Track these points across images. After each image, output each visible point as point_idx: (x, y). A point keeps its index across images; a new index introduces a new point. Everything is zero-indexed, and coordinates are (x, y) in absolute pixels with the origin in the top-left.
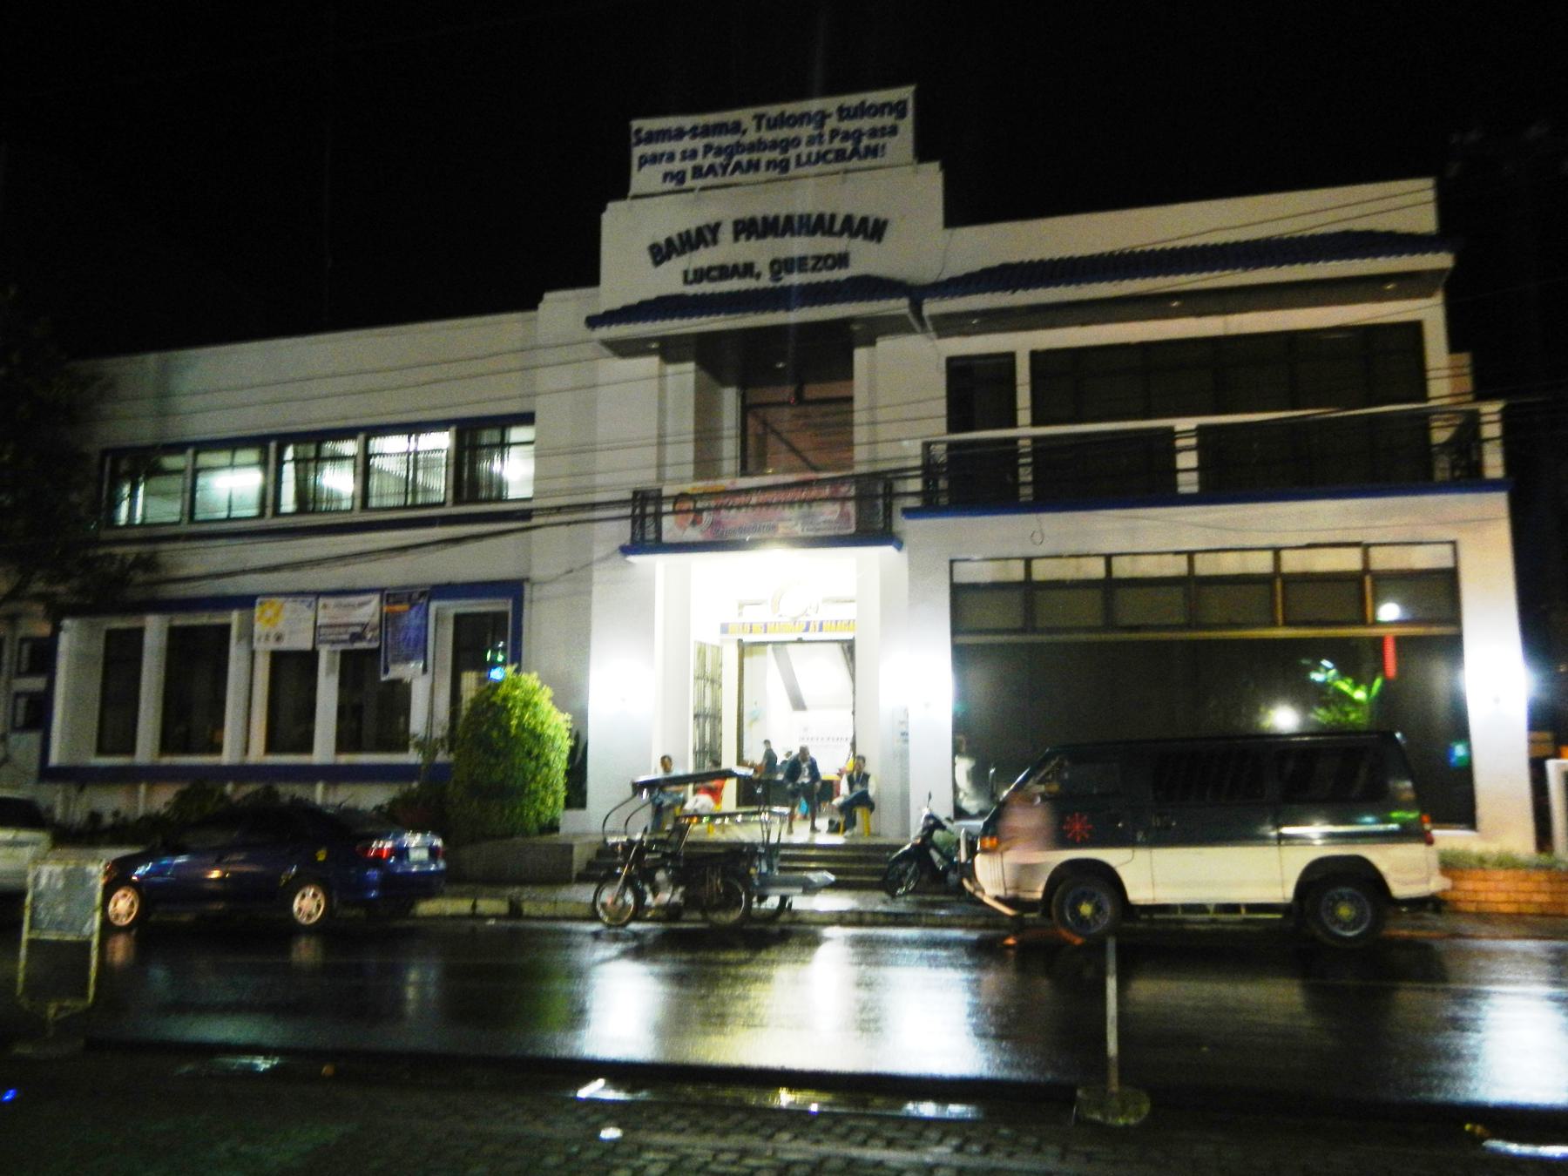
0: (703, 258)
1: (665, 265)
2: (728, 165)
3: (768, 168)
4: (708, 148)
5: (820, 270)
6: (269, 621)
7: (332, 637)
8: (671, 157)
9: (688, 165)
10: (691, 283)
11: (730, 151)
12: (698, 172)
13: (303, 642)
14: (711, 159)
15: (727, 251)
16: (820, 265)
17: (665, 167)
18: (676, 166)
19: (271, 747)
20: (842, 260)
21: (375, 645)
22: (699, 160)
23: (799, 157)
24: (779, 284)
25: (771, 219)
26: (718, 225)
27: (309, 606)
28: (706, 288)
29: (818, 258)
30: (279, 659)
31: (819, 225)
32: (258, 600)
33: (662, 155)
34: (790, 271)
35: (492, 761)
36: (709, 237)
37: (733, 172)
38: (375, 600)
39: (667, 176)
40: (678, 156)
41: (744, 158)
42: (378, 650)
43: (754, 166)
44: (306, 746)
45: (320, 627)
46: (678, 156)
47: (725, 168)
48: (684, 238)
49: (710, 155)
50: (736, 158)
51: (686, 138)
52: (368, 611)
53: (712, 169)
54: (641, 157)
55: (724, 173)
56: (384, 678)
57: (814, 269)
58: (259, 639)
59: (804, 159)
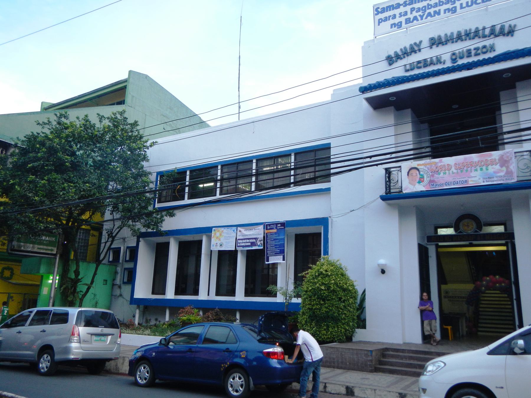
0: (414, 58)
1: (395, 65)
2: (424, 15)
3: (445, 13)
4: (412, 10)
5: (479, 54)
6: (217, 238)
8: (394, 17)
9: (403, 19)
10: (407, 71)
11: (424, 9)
12: (408, 21)
13: (230, 246)
14: (415, 14)
15: (426, 54)
16: (479, 52)
17: (392, 21)
18: (397, 21)
20: (492, 48)
21: (262, 248)
22: (409, 16)
23: (461, 4)
24: (455, 65)
25: (449, 34)
26: (421, 42)
27: (234, 231)
28: (416, 72)
29: (477, 49)
30: (222, 254)
31: (476, 34)
32: (213, 229)
33: (390, 16)
34: (461, 58)
36: (416, 48)
37: (426, 18)
38: (261, 227)
39: (392, 26)
40: (398, 16)
41: (432, 11)
43: (438, 13)
44: (232, 293)
45: (238, 239)
46: (398, 16)
47: (422, 17)
48: (404, 50)
49: (414, 12)
50: (428, 11)
51: (401, 7)
52: (259, 233)
53: (415, 18)
54: (379, 20)
55: (422, 19)
56: (266, 263)
57: (476, 55)
58: (213, 246)
59: (464, 5)
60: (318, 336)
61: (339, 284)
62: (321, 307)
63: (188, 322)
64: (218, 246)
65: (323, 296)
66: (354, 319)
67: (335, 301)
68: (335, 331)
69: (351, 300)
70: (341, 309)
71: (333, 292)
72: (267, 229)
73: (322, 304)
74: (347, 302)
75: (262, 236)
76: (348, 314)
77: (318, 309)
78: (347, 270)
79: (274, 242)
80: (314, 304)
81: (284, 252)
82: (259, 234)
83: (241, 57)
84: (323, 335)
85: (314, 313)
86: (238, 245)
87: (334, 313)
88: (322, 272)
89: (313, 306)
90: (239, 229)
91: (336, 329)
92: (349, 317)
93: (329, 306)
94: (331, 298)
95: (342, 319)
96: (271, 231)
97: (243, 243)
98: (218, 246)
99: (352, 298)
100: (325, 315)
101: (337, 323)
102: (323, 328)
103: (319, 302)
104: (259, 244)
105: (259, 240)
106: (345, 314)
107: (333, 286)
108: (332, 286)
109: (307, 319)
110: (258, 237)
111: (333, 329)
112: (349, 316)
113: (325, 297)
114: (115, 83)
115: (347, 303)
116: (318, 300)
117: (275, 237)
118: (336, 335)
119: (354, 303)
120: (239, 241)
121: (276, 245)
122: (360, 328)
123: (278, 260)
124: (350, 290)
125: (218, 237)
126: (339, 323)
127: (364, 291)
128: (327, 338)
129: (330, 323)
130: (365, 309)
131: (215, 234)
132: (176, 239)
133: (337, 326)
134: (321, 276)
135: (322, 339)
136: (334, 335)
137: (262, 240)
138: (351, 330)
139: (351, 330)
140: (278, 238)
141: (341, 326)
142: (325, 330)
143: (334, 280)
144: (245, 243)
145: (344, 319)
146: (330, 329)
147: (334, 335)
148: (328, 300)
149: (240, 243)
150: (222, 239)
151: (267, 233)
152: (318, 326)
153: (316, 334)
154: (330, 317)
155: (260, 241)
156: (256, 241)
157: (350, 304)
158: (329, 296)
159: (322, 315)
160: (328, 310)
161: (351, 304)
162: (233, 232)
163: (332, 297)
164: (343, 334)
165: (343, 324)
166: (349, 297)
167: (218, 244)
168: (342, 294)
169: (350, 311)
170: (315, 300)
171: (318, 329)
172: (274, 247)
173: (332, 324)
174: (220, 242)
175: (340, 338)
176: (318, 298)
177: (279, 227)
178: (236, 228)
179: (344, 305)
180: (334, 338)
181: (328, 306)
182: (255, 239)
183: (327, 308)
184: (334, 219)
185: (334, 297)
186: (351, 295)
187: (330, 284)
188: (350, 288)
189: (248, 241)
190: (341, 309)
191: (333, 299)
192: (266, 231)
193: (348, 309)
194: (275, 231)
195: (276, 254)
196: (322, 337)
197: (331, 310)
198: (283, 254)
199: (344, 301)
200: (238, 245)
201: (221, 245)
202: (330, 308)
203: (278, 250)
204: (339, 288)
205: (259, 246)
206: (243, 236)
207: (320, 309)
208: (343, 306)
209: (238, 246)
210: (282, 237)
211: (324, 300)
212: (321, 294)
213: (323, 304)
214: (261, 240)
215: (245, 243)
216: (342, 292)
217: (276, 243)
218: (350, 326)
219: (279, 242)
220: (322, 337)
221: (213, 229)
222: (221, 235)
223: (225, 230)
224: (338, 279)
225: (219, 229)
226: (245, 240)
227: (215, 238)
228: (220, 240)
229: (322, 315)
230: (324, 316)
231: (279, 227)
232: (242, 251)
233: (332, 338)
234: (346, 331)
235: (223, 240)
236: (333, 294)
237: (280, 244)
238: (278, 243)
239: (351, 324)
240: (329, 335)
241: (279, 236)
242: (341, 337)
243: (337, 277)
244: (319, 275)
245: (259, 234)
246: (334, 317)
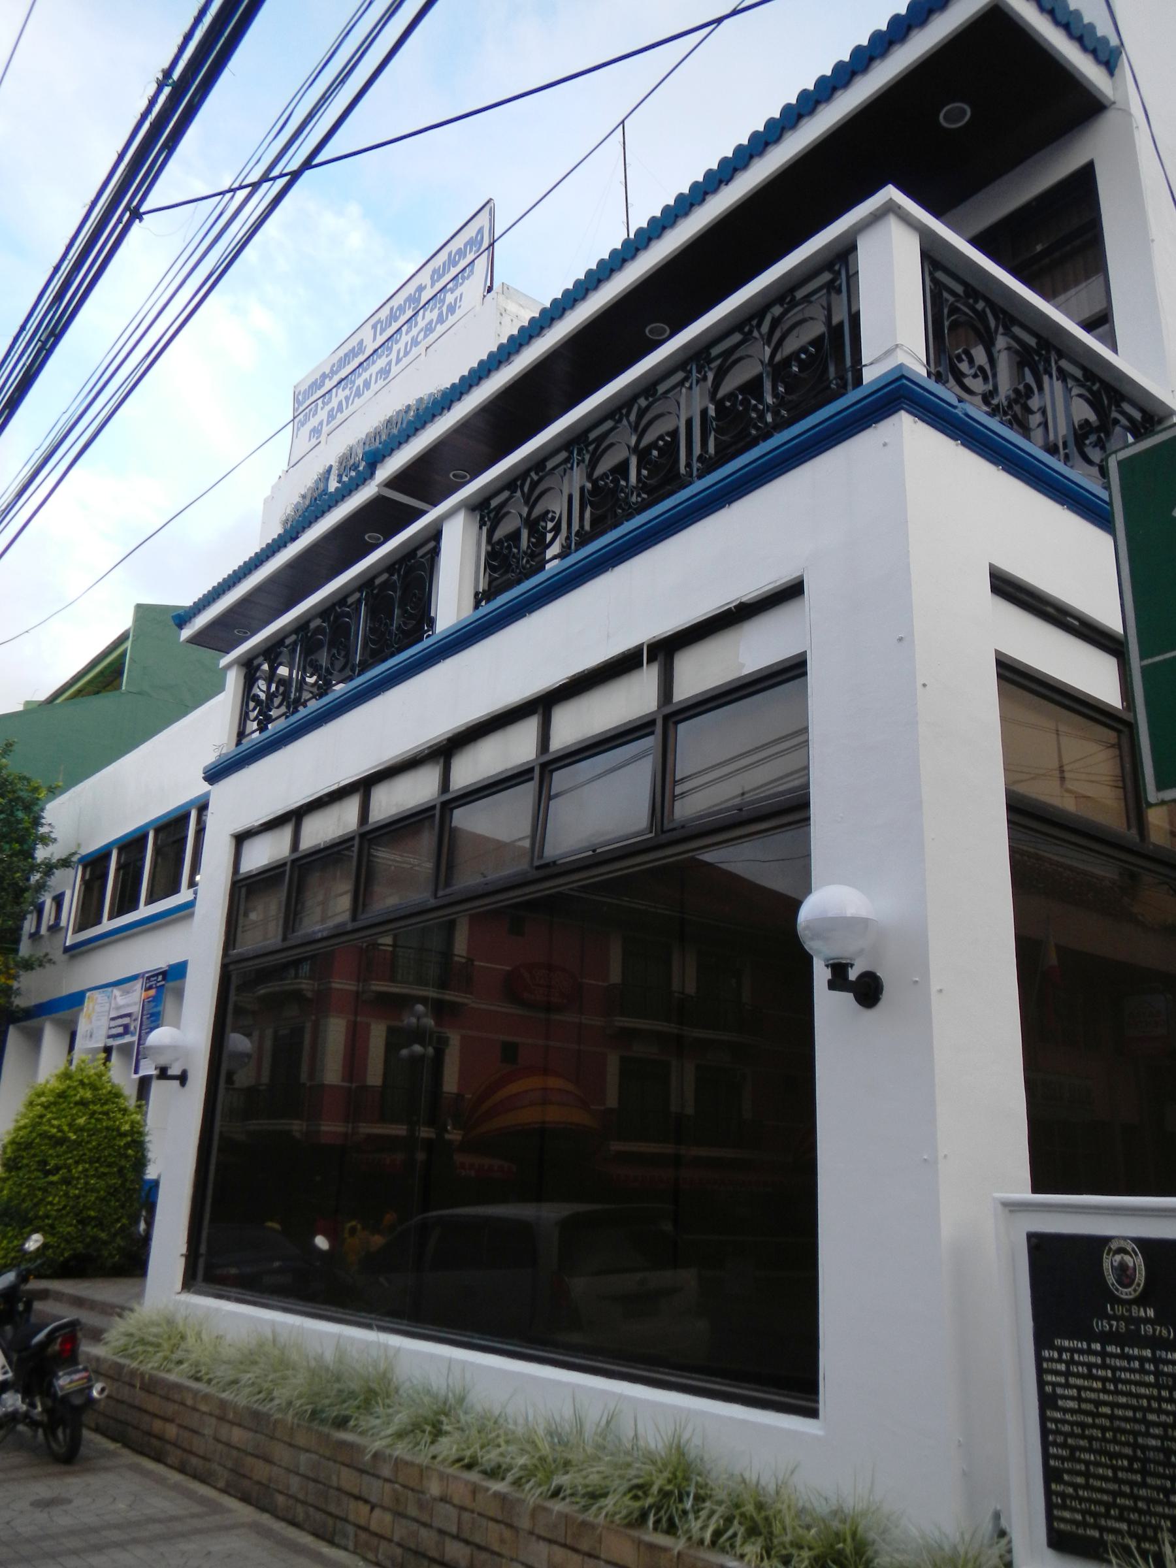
32: (88, 994)
38: (138, 985)
182: (129, 1015)
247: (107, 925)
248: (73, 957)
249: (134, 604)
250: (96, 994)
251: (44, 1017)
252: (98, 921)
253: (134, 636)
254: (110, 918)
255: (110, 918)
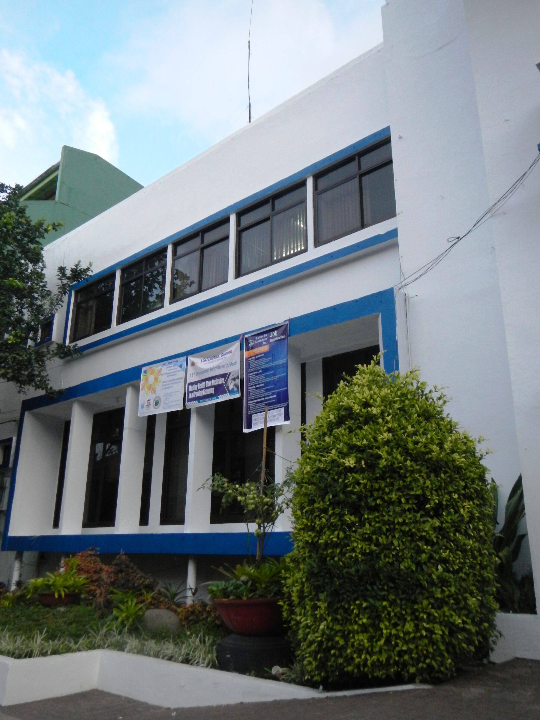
6: (150, 387)
7: (199, 394)
19: (165, 520)
21: (238, 396)
27: (181, 366)
35: (349, 518)
42: (240, 400)
45: (189, 384)
58: (142, 408)
60: (341, 656)
61: (410, 446)
62: (347, 537)
63: (45, 592)
64: (152, 406)
65: (352, 492)
66: (483, 582)
67: (398, 509)
68: (407, 633)
69: (467, 504)
70: (428, 542)
71: (391, 477)
72: (248, 349)
73: (350, 526)
74: (449, 514)
75: (237, 367)
76: (457, 560)
77: (336, 545)
78: (445, 402)
79: (262, 376)
80: (322, 529)
81: (286, 399)
82: (231, 364)
83: (251, 105)
84: (359, 652)
85: (323, 560)
86: (190, 397)
87: (399, 559)
88: (349, 409)
89: (320, 533)
90: (191, 359)
91: (409, 627)
92: (461, 574)
93: (378, 532)
94: (382, 499)
95: (432, 583)
96: (257, 350)
97: (198, 390)
98: (152, 406)
99: (470, 498)
100: (362, 567)
101: (415, 602)
102: (356, 623)
103: (340, 520)
104: (231, 387)
105: (231, 377)
106: (444, 561)
107: (389, 454)
108: (383, 452)
109: (303, 583)
110: (229, 372)
111: (395, 625)
112: (460, 569)
113: (360, 497)
114: (45, 172)
115: (448, 517)
116: (337, 511)
117: (266, 363)
118: (409, 652)
119: (480, 519)
120: (190, 386)
121: (267, 384)
122: (515, 612)
123: (274, 420)
124: (458, 469)
125: (151, 385)
126: (420, 598)
127: (518, 485)
128: (373, 664)
129: (384, 599)
130: (525, 539)
131: (147, 380)
132: (85, 405)
133: (413, 613)
134: (349, 423)
135: (358, 666)
136: (401, 654)
137: (238, 378)
138: (473, 629)
139: (473, 629)
140: (271, 364)
141: (429, 615)
142: (364, 629)
143: (389, 430)
144: (202, 389)
145: (443, 582)
146: (382, 626)
147: (405, 652)
148: (376, 508)
149: (192, 392)
150: (159, 387)
151: (247, 359)
152: (341, 611)
153: (333, 647)
154: (381, 576)
155: (234, 379)
156: (226, 383)
157: (462, 521)
158: (375, 494)
159: (353, 570)
160: (373, 547)
161: (469, 522)
162: (179, 369)
163: (386, 498)
164: (442, 648)
165: (440, 604)
166: (456, 496)
167: (152, 401)
168: (428, 483)
169: (464, 551)
170: (325, 511)
171: (337, 627)
172: (263, 390)
173: (392, 603)
174: (154, 396)
175: (430, 666)
176: (334, 504)
177: (275, 337)
178: (185, 358)
179: (438, 524)
180: (405, 665)
181: (374, 533)
182: (224, 376)
183: (368, 539)
184: (410, 291)
185: (394, 496)
186: (465, 487)
187: (378, 448)
188: (459, 459)
189: (208, 383)
190: (428, 542)
191: (391, 502)
192: (245, 354)
193: (455, 541)
194: (265, 348)
195: (271, 405)
196: (357, 660)
197: (388, 547)
198: (285, 404)
199: (437, 512)
200: (190, 397)
201: (156, 404)
202: (382, 540)
203: (273, 394)
204: (414, 459)
205: (231, 392)
206: (198, 374)
207: (342, 544)
208: (434, 529)
209: (189, 400)
210: (281, 361)
211: (356, 510)
212: (346, 486)
213: (353, 524)
214: (235, 376)
215: (202, 389)
216: (428, 477)
217: (268, 379)
218: (470, 611)
219: (274, 375)
220: (357, 660)
221: (143, 370)
222: (156, 379)
223: (164, 368)
224: (410, 429)
225: (154, 366)
226: (204, 383)
227: (146, 389)
228: (155, 392)
229: (353, 570)
230: (357, 571)
231: (273, 338)
232: (200, 411)
233: (396, 663)
234: (452, 633)
235: (160, 392)
236: (392, 484)
237: (279, 378)
238: (272, 379)
239: (472, 601)
240: (380, 652)
241: (273, 360)
242: (433, 658)
243: (404, 422)
244: (340, 422)
245: (231, 364)
246: (399, 573)
247: (115, 328)
248: (68, 362)
249: (62, 146)
250: (156, 367)
251: (72, 400)
252: (108, 325)
253: (63, 166)
254: (119, 323)
255: (119, 323)
